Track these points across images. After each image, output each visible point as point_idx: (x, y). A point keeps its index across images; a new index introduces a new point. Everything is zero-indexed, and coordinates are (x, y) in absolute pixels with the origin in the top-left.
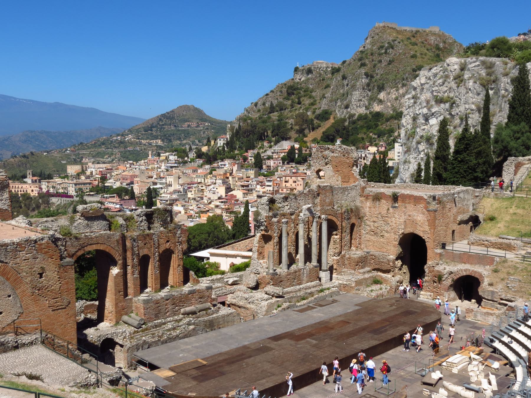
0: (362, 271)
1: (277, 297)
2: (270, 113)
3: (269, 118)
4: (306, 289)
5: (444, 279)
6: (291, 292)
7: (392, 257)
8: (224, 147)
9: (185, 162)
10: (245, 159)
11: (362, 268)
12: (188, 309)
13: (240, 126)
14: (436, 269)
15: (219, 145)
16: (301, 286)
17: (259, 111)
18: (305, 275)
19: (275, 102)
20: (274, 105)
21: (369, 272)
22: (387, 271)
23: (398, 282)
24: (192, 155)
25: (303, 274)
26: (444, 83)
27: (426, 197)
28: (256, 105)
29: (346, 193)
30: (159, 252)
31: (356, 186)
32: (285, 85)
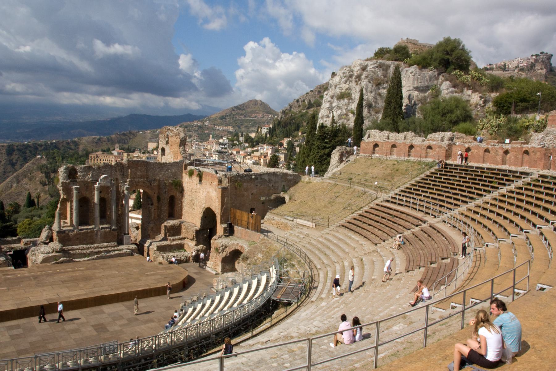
1: (57, 252)
2: (309, 108)
3: (307, 112)
4: (96, 248)
5: (220, 251)
6: (77, 249)
7: (197, 228)
8: (266, 134)
9: (234, 145)
10: (281, 145)
13: (281, 118)
14: (217, 241)
15: (263, 133)
17: (299, 106)
18: (99, 236)
19: (313, 101)
20: (312, 102)
21: (179, 239)
24: (242, 139)
25: (97, 234)
26: (346, 82)
28: (298, 101)
32: (323, 86)
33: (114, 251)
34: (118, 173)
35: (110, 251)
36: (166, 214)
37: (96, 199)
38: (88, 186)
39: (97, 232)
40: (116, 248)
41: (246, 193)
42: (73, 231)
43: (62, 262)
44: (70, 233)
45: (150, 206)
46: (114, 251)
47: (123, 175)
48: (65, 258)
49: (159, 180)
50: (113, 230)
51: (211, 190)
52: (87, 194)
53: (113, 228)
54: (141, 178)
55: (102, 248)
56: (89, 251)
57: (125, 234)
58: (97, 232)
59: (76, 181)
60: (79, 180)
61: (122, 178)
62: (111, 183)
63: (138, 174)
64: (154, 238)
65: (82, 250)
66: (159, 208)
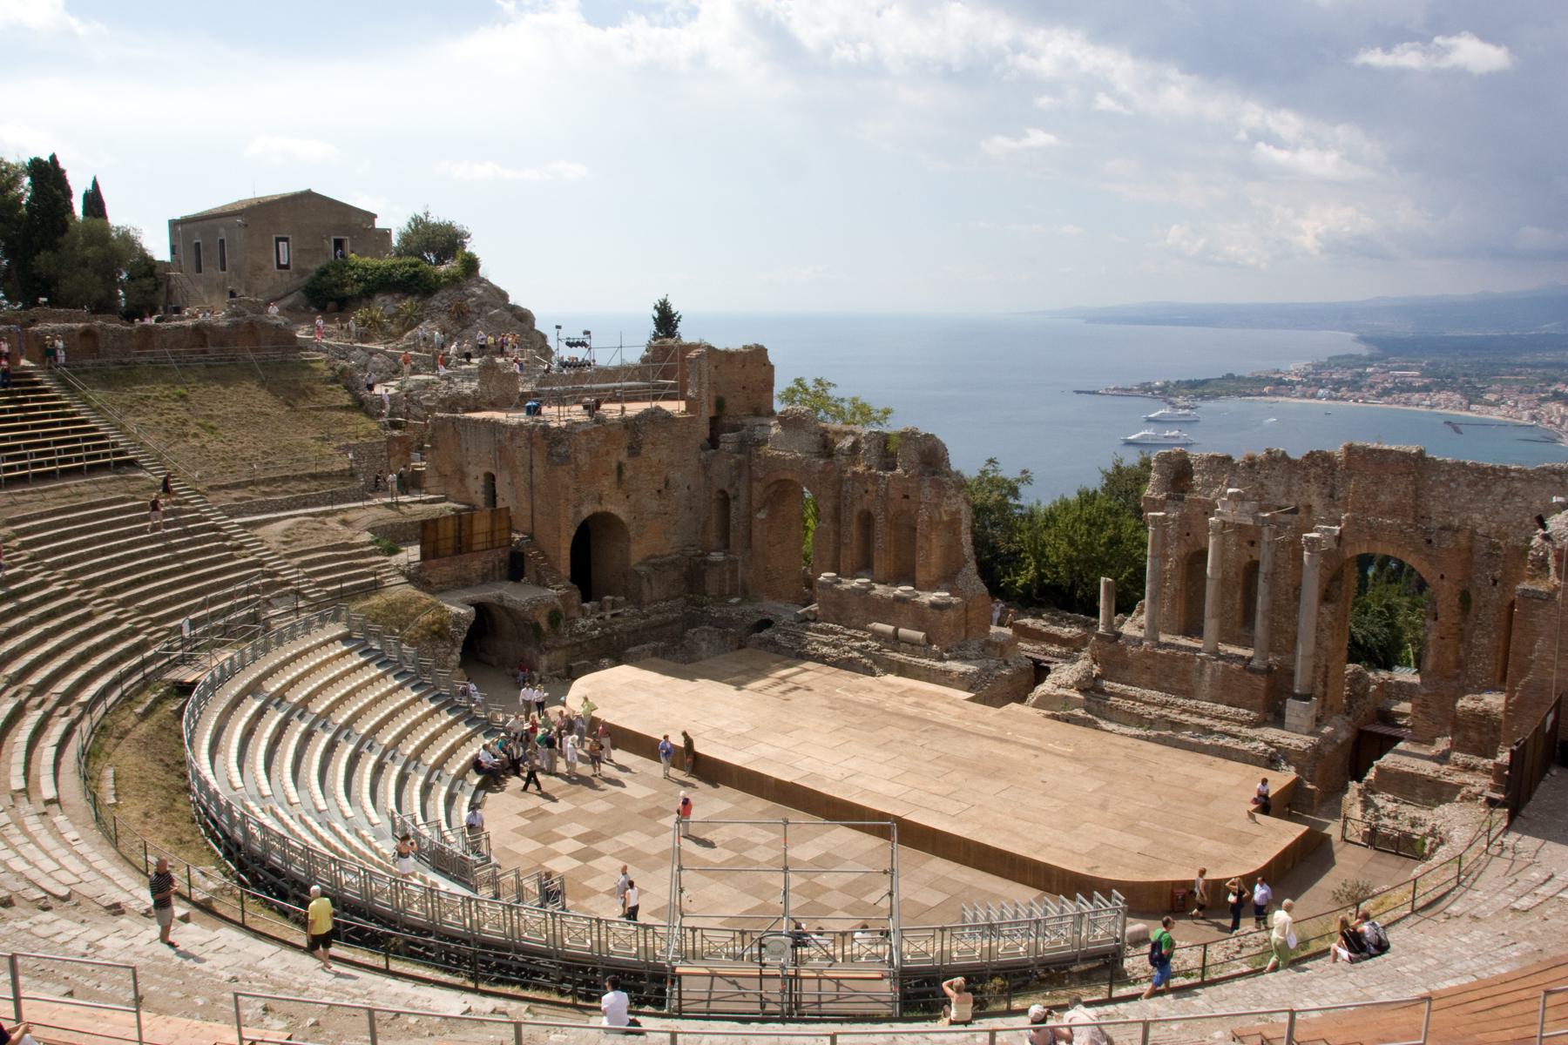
4: (1184, 711)
16: (1180, 701)
18: (1207, 678)
29: (1500, 490)
30: (886, 510)
33: (1225, 734)
34: (1314, 488)
35: (1207, 731)
39: (1203, 664)
40: (1235, 729)
42: (1140, 641)
43: (1067, 720)
44: (1129, 648)
46: (1225, 734)
47: (1331, 496)
48: (1080, 712)
49: (1473, 532)
50: (1254, 671)
53: (1255, 663)
54: (1393, 512)
55: (1202, 716)
56: (1155, 712)
58: (1203, 664)
59: (1182, 499)
60: (1193, 496)
61: (1327, 507)
62: (1256, 519)
63: (1383, 498)
64: (1432, 743)
65: (1146, 703)
66: (1462, 636)
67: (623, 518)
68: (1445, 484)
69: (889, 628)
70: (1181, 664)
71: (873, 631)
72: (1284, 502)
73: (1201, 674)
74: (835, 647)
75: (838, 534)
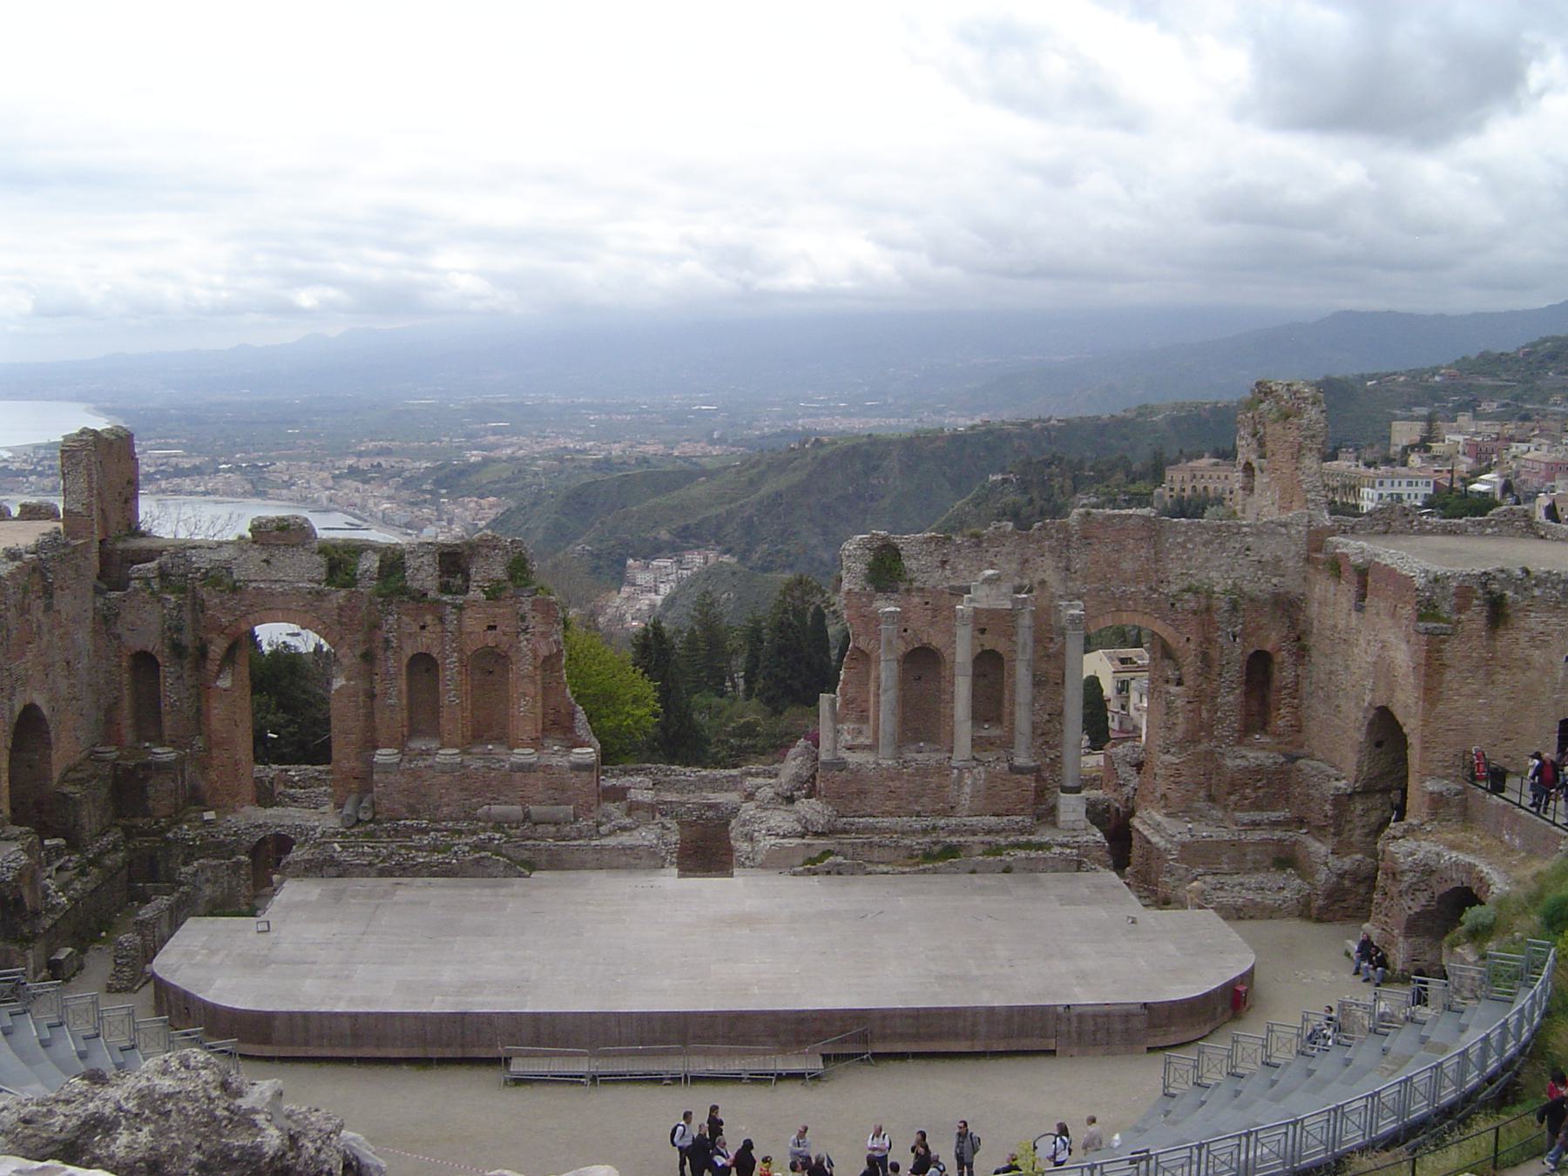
0: (1246, 817)
7: (1342, 784)
11: (1257, 806)
12: (497, 809)
16: (942, 822)
18: (967, 790)
21: (1275, 824)
22: (1319, 831)
23: (1341, 876)
27: (1420, 582)
31: (1285, 525)
34: (1049, 561)
36: (1235, 721)
37: (962, 652)
38: (940, 606)
39: (961, 776)
41: (1537, 655)
45: (1173, 689)
47: (1068, 569)
51: (1392, 639)
52: (937, 641)
57: (1065, 790)
61: (1065, 580)
63: (1124, 565)
67: (45, 712)
68: (1183, 546)
69: (516, 810)
70: (934, 781)
71: (489, 817)
72: (1017, 581)
73: (960, 787)
74: (435, 849)
75: (371, 696)
